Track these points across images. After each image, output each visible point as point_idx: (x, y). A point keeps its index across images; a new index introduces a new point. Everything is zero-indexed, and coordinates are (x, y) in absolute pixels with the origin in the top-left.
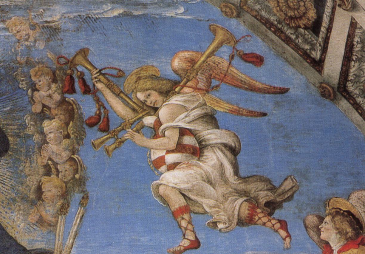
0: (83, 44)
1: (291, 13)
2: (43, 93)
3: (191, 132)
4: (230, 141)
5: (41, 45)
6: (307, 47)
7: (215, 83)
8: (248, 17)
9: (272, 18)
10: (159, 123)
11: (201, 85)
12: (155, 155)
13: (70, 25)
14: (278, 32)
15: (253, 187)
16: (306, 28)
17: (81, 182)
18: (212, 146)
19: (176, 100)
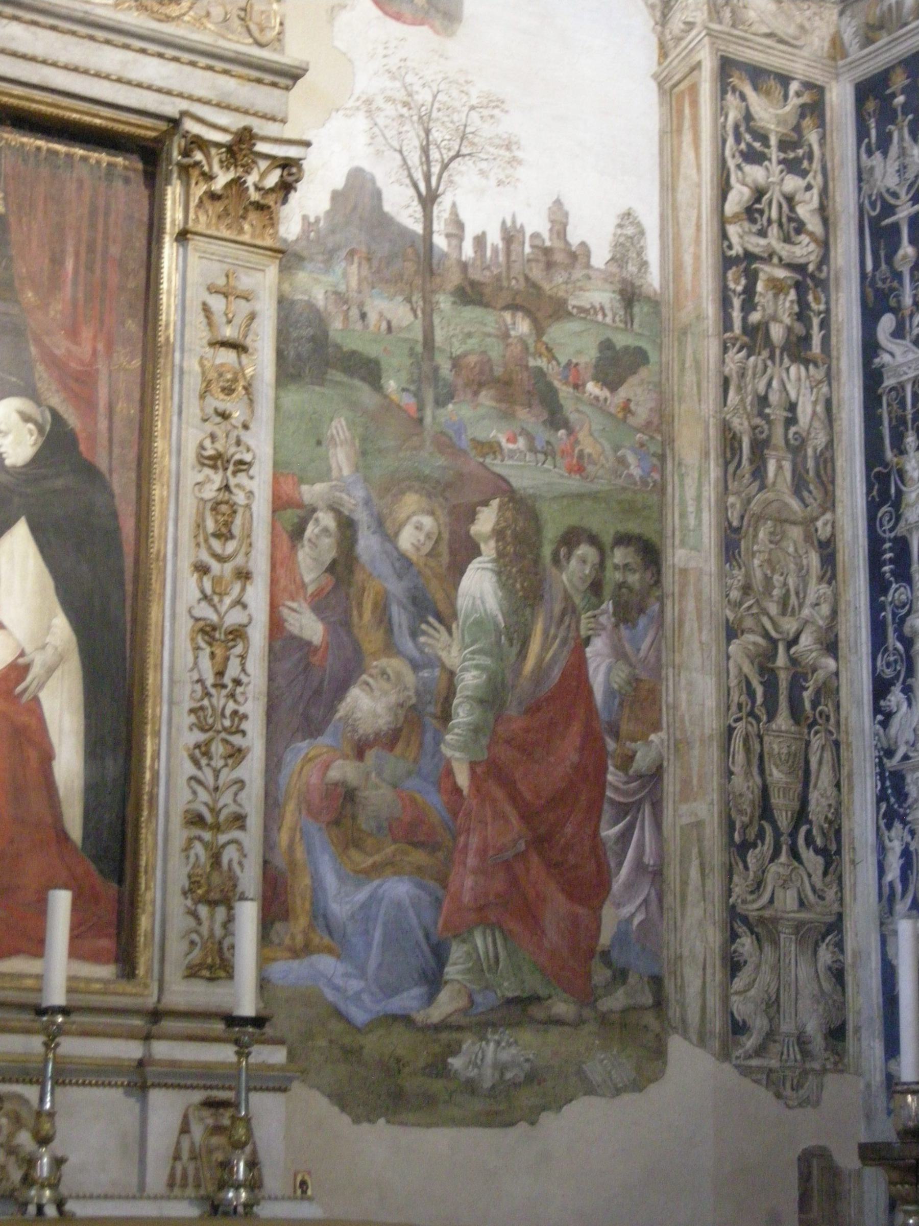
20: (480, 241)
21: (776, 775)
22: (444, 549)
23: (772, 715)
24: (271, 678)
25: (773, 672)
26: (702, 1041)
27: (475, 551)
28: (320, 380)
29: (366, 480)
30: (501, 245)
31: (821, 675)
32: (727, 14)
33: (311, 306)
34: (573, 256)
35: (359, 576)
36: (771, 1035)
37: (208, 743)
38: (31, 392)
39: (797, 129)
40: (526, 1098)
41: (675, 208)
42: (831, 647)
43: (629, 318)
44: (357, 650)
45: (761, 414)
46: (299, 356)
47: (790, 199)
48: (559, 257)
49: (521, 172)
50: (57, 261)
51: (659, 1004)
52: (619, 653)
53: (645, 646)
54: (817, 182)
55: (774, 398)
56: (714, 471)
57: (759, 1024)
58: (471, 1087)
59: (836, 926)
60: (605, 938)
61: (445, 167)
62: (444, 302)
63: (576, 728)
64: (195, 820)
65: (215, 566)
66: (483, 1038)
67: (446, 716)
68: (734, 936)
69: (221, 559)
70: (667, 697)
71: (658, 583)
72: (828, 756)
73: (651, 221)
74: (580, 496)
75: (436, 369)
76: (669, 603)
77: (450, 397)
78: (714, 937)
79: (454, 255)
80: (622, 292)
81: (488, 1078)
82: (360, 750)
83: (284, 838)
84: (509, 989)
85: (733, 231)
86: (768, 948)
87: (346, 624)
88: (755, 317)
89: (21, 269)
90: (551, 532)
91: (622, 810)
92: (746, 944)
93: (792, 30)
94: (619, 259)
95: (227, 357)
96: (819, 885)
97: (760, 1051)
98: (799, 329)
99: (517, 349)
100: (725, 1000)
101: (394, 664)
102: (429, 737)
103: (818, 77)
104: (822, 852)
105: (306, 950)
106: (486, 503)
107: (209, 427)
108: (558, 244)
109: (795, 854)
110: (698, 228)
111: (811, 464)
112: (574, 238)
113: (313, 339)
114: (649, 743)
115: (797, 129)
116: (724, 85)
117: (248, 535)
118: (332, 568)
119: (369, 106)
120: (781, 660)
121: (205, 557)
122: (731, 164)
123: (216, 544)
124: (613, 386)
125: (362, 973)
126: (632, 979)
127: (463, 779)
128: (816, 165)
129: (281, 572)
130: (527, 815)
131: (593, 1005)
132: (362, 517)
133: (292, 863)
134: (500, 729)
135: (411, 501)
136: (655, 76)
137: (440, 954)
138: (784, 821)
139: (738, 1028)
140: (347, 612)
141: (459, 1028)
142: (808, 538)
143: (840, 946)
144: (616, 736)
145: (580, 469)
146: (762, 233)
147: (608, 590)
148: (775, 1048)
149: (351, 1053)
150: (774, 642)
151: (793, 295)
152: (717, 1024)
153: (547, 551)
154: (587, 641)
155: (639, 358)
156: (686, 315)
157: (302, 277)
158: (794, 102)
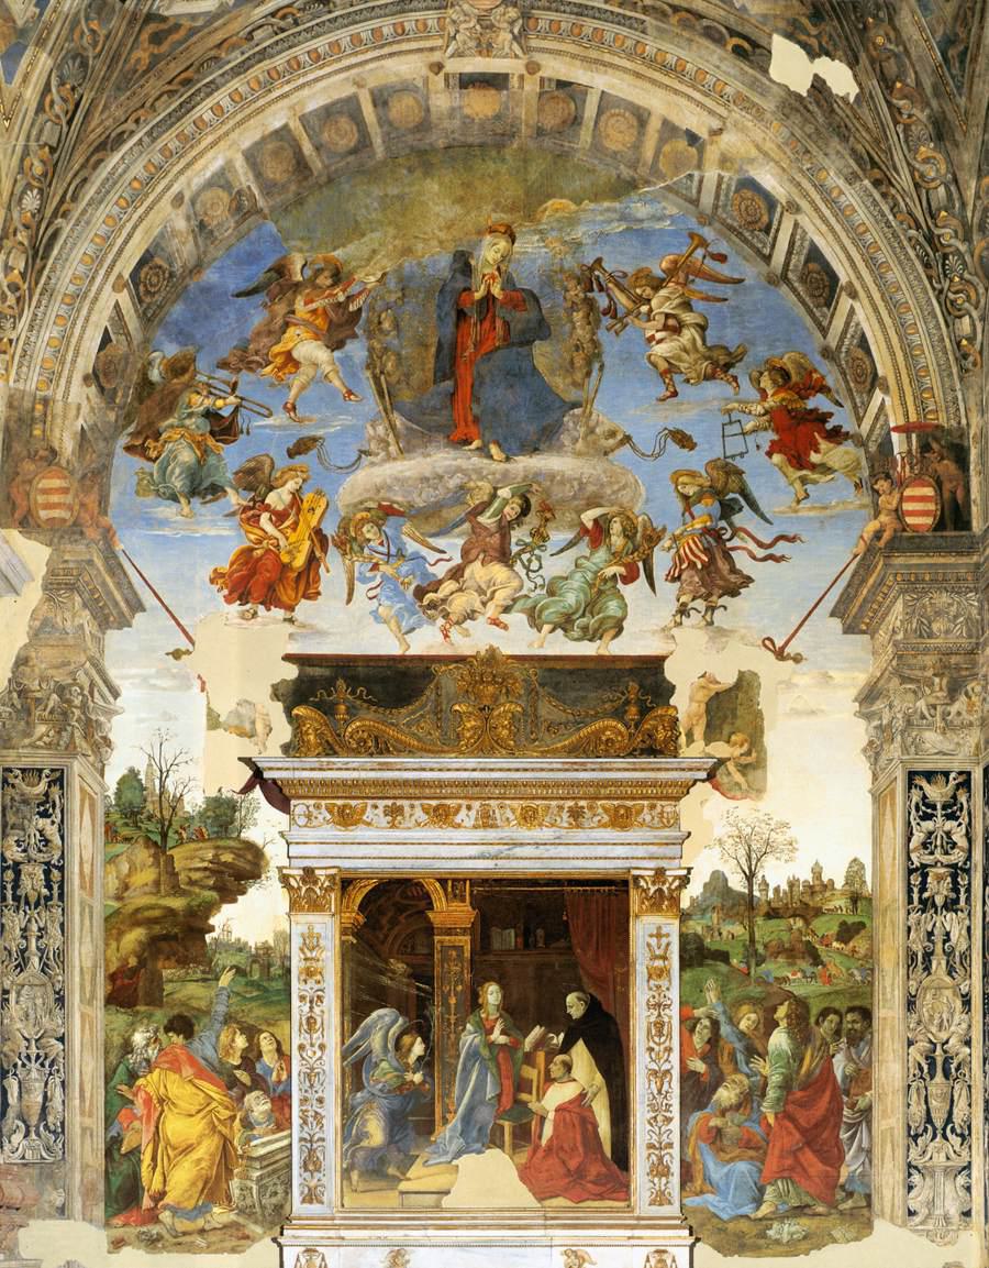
0: (599, 255)
1: (749, 219)
2: (572, 293)
3: (674, 316)
4: (699, 320)
5: (569, 257)
6: (760, 246)
7: (691, 277)
8: (717, 225)
9: (735, 224)
10: (651, 310)
11: (681, 280)
12: (649, 334)
13: (589, 241)
14: (739, 235)
15: (715, 354)
16: (760, 230)
17: (598, 356)
18: (688, 326)
19: (663, 292)
20: (777, 890)
21: (934, 1103)
22: (761, 1026)
23: (932, 1078)
24: (681, 1088)
25: (934, 1059)
26: (892, 1220)
27: (777, 1025)
28: (701, 965)
29: (724, 1003)
30: (787, 888)
31: (961, 1056)
32: (913, 749)
33: (696, 934)
34: (825, 887)
35: (721, 1043)
36: (929, 1216)
37: (655, 1117)
38: (580, 989)
39: (954, 797)
40: (804, 1245)
41: (881, 852)
42: (968, 1043)
43: (855, 907)
44: (722, 1073)
45: (929, 940)
46: (691, 957)
47: (948, 834)
48: (817, 889)
49: (797, 854)
50: (590, 934)
51: (869, 1205)
52: (849, 1059)
53: (864, 1054)
54: (964, 820)
55: (936, 932)
56: (902, 971)
57: (924, 1212)
58: (778, 1242)
59: (968, 1167)
60: (842, 1180)
61: (759, 860)
62: (759, 921)
63: (828, 1094)
64: (651, 1146)
65: (656, 1048)
66: (783, 1222)
67: (763, 1095)
68: (910, 1175)
69: (659, 1044)
70: (875, 1076)
71: (870, 1025)
72: (964, 1092)
73: (867, 861)
74: (829, 994)
75: (756, 951)
76: (876, 1035)
77: (763, 961)
78: (900, 1176)
79: (764, 898)
80: (851, 898)
81: (785, 1238)
82: (723, 1113)
83: (690, 1151)
84: (795, 1202)
85: (914, 856)
86: (928, 1179)
87: (717, 1064)
88: (926, 895)
89: (575, 941)
90: (814, 1011)
91: (850, 1126)
92: (916, 1178)
93: (952, 747)
94: (849, 881)
95: (659, 963)
96: (957, 1148)
97: (922, 1223)
98: (953, 895)
99: (797, 934)
100: (905, 1201)
101: (738, 1077)
102: (755, 1105)
103: (967, 768)
104: (962, 1136)
105: (702, 1192)
106: (782, 1004)
107: (651, 993)
108: (817, 882)
109: (945, 1137)
110: (894, 858)
111: (957, 960)
112: (825, 879)
113: (697, 949)
114: (864, 1096)
115: (954, 797)
116: (910, 784)
117: (670, 1034)
118: (709, 1042)
119: (720, 842)
120: (939, 1051)
121: (652, 1044)
122: (913, 823)
123: (656, 1039)
124: (846, 943)
125: (726, 1200)
126: (855, 1196)
127: (771, 1120)
128: (965, 812)
129: (685, 1047)
130: (803, 1132)
131: (836, 1207)
132: (722, 1019)
133: (694, 1160)
134: (790, 1097)
135: (745, 1008)
136: (870, 791)
137: (762, 1191)
138: (939, 1124)
139: (911, 1213)
140: (717, 1058)
141: (771, 1219)
142: (954, 994)
143: (969, 1176)
144: (848, 1096)
145: (829, 982)
146: (932, 853)
147: (844, 1032)
148: (931, 1221)
149: (724, 1231)
150: (935, 1045)
151: (949, 879)
152: (901, 1212)
153: (812, 1020)
154: (833, 1056)
155: (862, 926)
156: (885, 903)
157: (691, 923)
158: (952, 783)
